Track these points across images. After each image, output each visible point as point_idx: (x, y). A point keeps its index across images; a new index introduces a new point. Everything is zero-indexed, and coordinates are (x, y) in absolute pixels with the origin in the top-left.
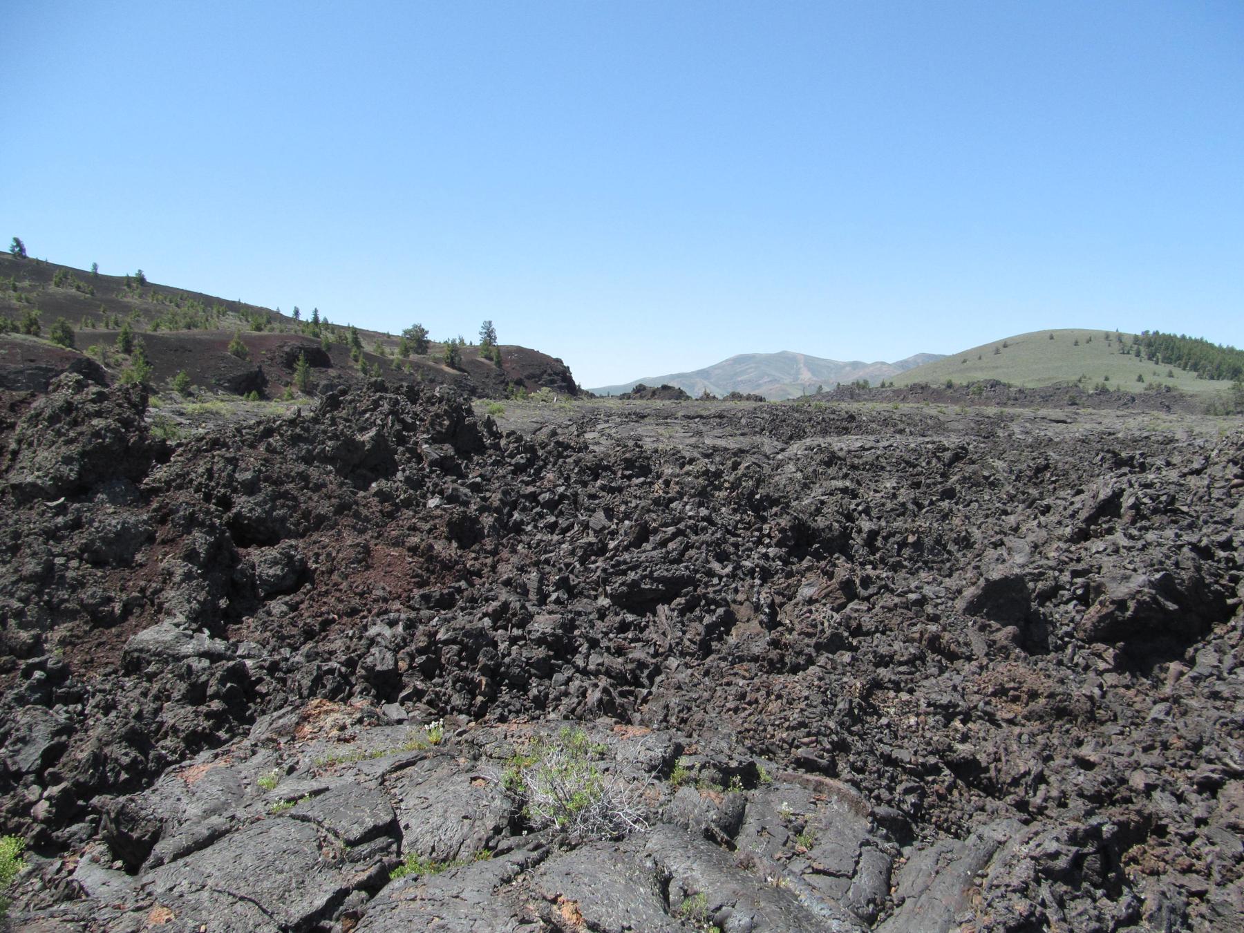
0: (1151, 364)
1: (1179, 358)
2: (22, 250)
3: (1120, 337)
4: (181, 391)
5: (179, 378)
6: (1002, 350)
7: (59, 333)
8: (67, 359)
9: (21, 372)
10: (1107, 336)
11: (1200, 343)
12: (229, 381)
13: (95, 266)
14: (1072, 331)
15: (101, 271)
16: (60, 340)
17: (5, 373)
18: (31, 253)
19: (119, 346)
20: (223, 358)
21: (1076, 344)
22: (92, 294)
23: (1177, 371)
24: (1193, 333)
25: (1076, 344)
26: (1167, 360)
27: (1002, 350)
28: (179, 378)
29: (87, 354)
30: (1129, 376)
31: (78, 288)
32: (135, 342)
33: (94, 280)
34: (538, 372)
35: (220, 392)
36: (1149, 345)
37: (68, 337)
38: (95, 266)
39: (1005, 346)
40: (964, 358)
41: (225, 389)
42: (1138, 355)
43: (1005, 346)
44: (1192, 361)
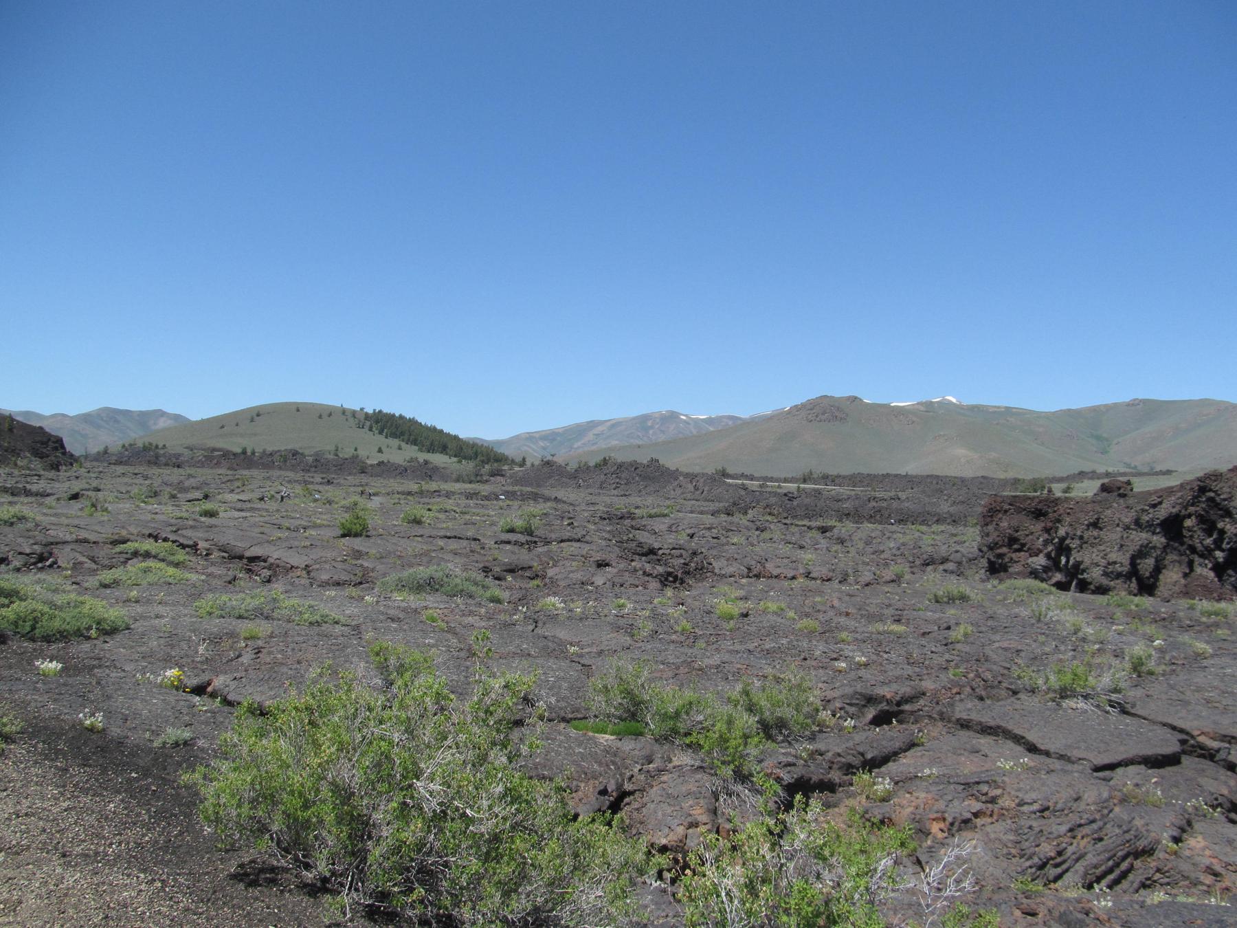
0: (382, 438)
1: (402, 434)
3: (354, 413)
6: (256, 418)
10: (344, 411)
11: (413, 422)
14: (313, 405)
21: (320, 417)
23: (403, 445)
24: (408, 415)
25: (320, 417)
26: (394, 435)
27: (256, 418)
30: (371, 448)
34: (45, 440)
36: (377, 422)
39: (258, 415)
40: (221, 424)
42: (371, 430)
43: (258, 415)
44: (412, 438)
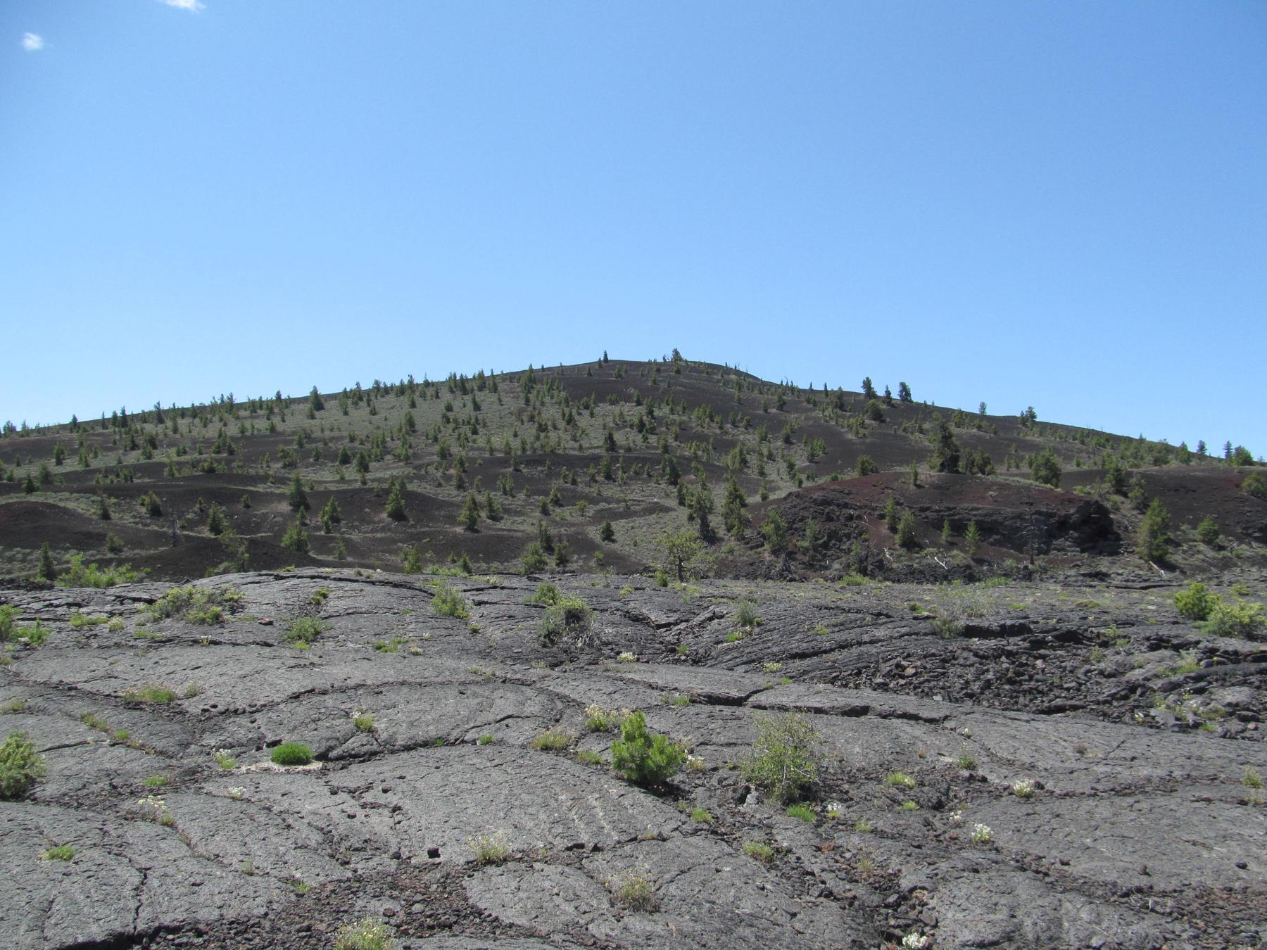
2: (908, 394)
4: (1208, 542)
5: (1205, 525)
7: (1043, 473)
8: (1070, 501)
9: (1019, 516)
12: (1260, 530)
13: (983, 407)
15: (989, 412)
16: (1047, 480)
17: (1000, 519)
18: (916, 397)
19: (1107, 486)
20: (1243, 500)
22: (995, 433)
28: (1205, 525)
29: (1078, 491)
31: (979, 428)
32: (1133, 481)
33: (981, 420)
35: (1254, 545)
37: (1054, 475)
38: (983, 407)
41: (1257, 539)
